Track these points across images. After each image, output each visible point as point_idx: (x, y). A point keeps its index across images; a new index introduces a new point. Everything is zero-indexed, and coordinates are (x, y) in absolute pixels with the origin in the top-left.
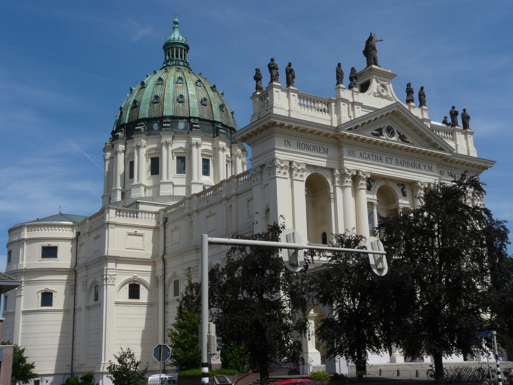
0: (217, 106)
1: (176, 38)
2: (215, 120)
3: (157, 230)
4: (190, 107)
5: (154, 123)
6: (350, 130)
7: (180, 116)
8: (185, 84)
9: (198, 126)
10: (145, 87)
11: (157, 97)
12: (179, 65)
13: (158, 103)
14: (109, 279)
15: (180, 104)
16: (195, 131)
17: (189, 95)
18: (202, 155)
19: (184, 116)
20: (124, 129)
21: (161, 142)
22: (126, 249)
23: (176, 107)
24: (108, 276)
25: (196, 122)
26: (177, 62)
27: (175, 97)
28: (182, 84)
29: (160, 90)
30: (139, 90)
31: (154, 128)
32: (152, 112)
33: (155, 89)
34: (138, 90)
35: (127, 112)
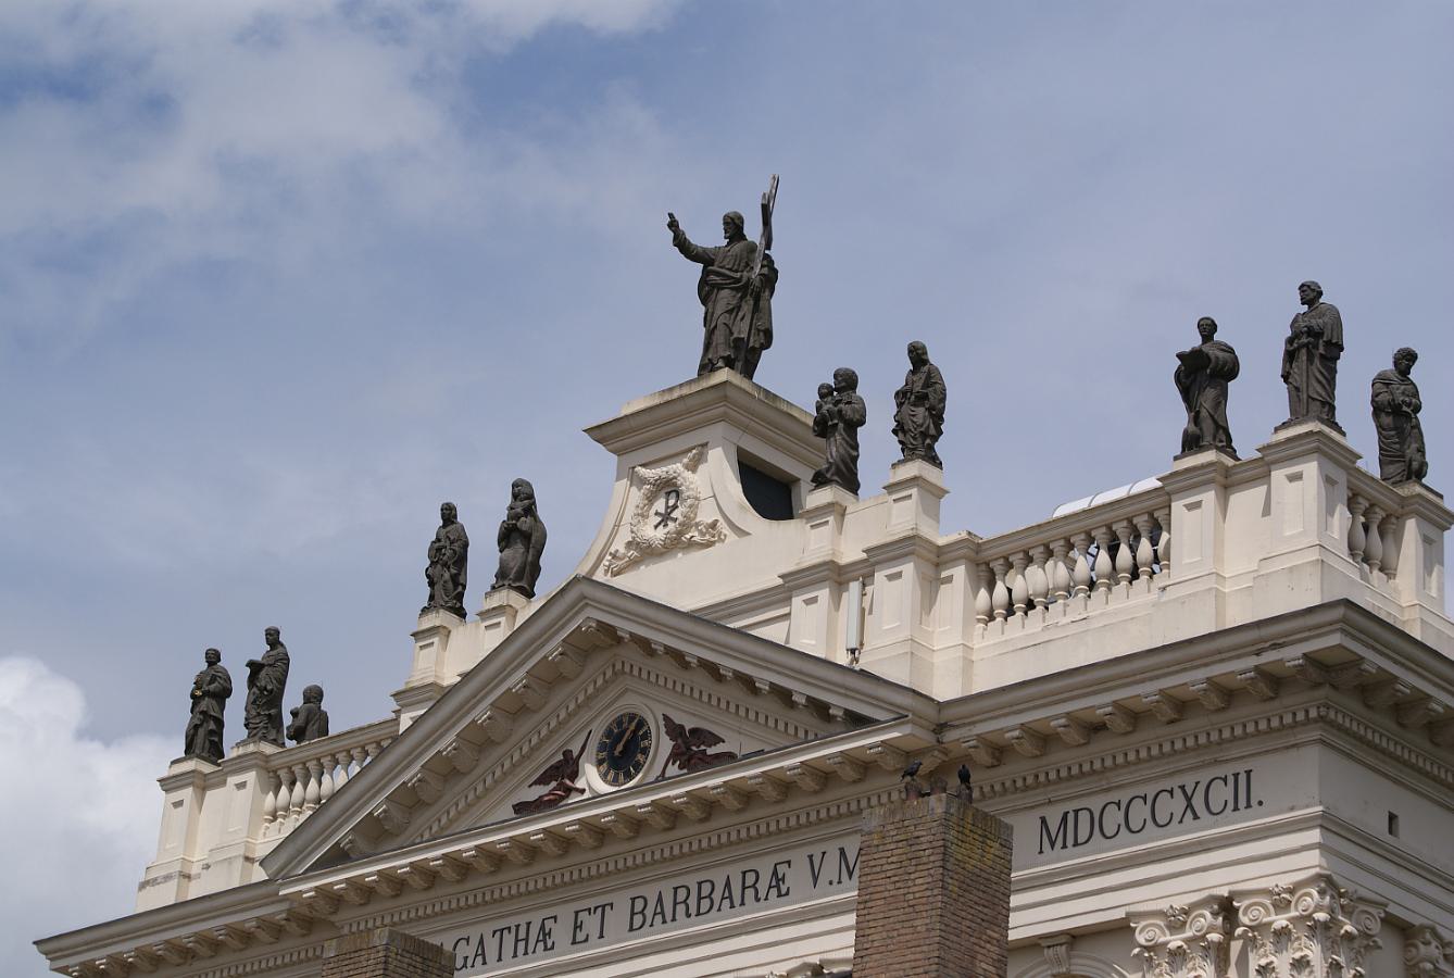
6: (339, 857)
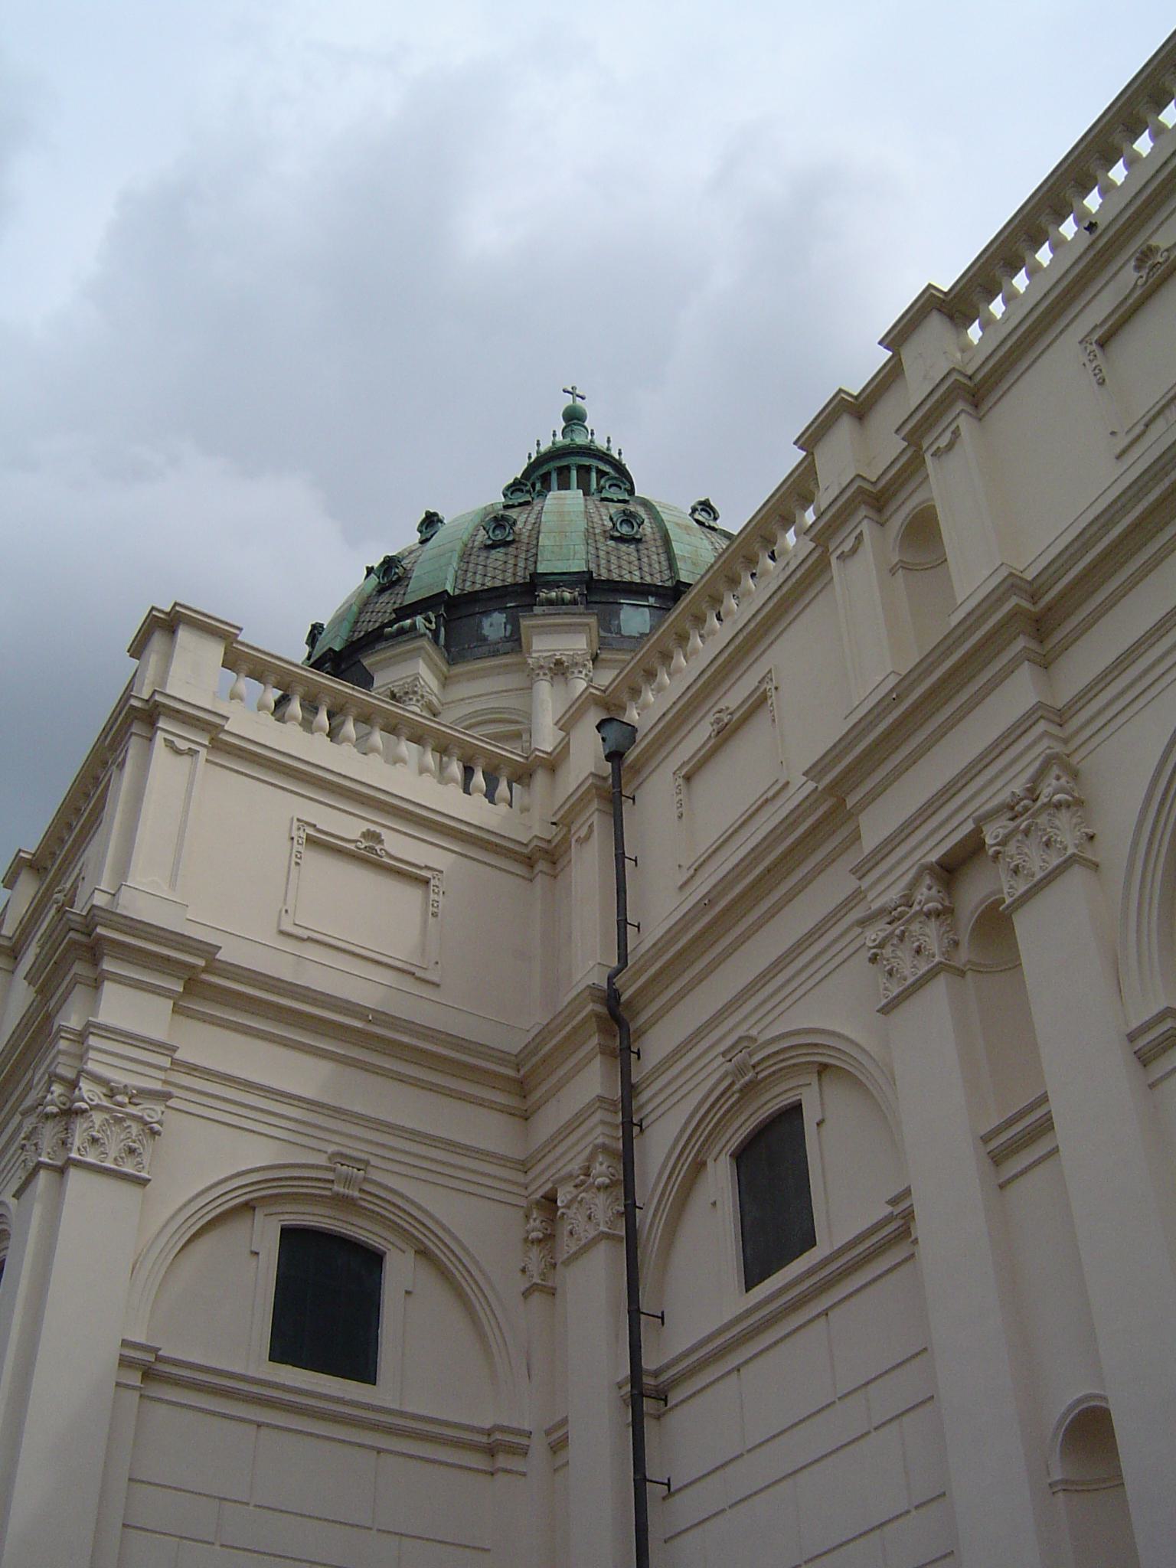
3: (542, 866)
5: (486, 613)
13: (506, 544)
14: (98, 1118)
15: (623, 547)
21: (530, 661)
22: (282, 933)
24: (86, 1087)
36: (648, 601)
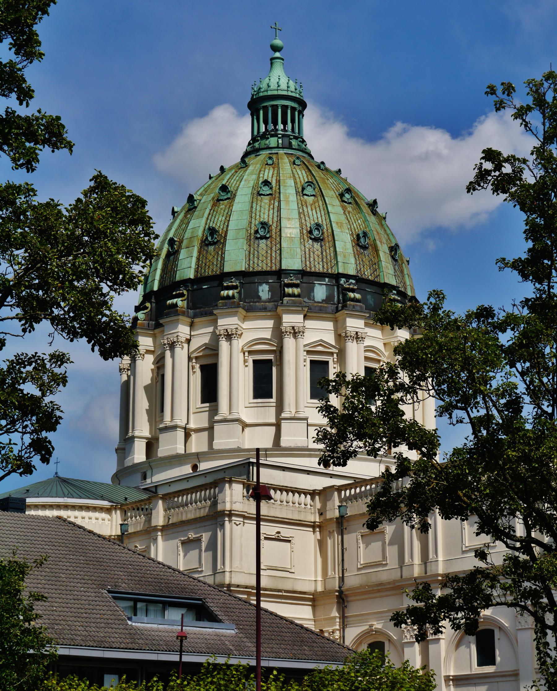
0: (387, 251)
1: (283, 85)
2: (387, 281)
4: (338, 252)
5: (261, 284)
7: (317, 270)
8: (319, 198)
9: (358, 296)
10: (228, 198)
11: (264, 225)
12: (290, 147)
13: (267, 238)
15: (315, 244)
16: (354, 307)
17: (334, 225)
18: (367, 359)
19: (325, 270)
20: (188, 291)
21: (282, 328)
23: (307, 250)
25: (351, 286)
26: (286, 140)
27: (304, 227)
28: (313, 197)
29: (267, 209)
30: (214, 205)
31: (261, 294)
32: (256, 259)
33: (254, 205)
34: (212, 203)
35: (192, 253)
36: (325, 281)
